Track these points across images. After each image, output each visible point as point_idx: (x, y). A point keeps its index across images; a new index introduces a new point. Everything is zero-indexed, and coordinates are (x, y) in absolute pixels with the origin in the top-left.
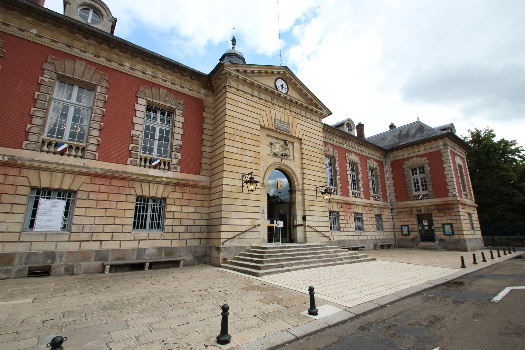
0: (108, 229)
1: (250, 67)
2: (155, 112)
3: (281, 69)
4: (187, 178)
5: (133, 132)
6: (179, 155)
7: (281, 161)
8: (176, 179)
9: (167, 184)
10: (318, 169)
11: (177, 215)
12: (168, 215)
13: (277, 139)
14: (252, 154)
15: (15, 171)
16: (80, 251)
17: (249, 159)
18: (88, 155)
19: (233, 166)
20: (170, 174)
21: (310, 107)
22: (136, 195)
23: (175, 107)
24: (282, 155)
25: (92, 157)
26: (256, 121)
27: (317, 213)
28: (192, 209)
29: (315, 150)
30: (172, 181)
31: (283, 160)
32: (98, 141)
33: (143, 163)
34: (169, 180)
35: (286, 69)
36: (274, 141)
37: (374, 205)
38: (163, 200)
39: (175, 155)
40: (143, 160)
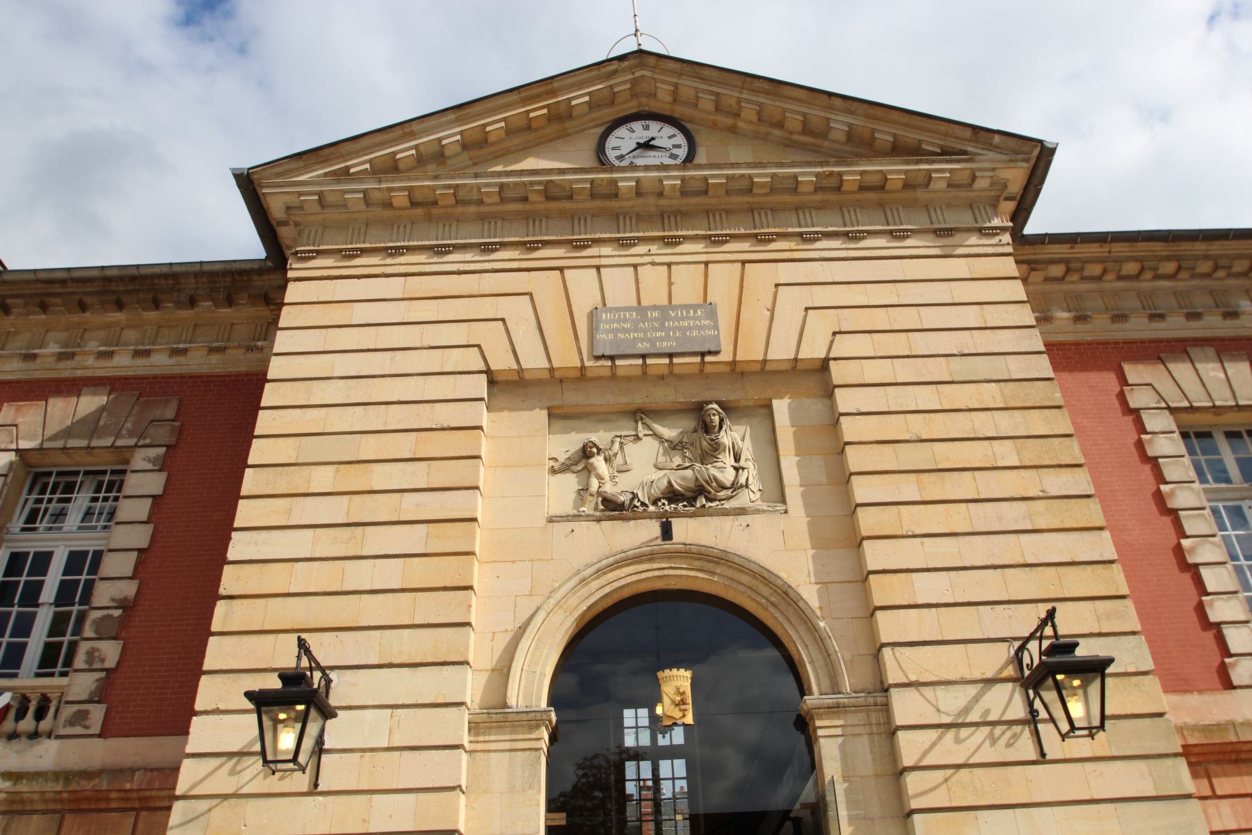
1: (413, 135)
2: (70, 488)
3: (615, 72)
6: (111, 651)
7: (667, 533)
8: (57, 775)
10: (1013, 515)
17: (390, 574)
19: (271, 637)
21: (852, 173)
23: (132, 442)
24: (672, 495)
26: (454, 360)
30: (36, 786)
31: (678, 526)
34: (23, 787)
35: (642, 66)
39: (91, 655)
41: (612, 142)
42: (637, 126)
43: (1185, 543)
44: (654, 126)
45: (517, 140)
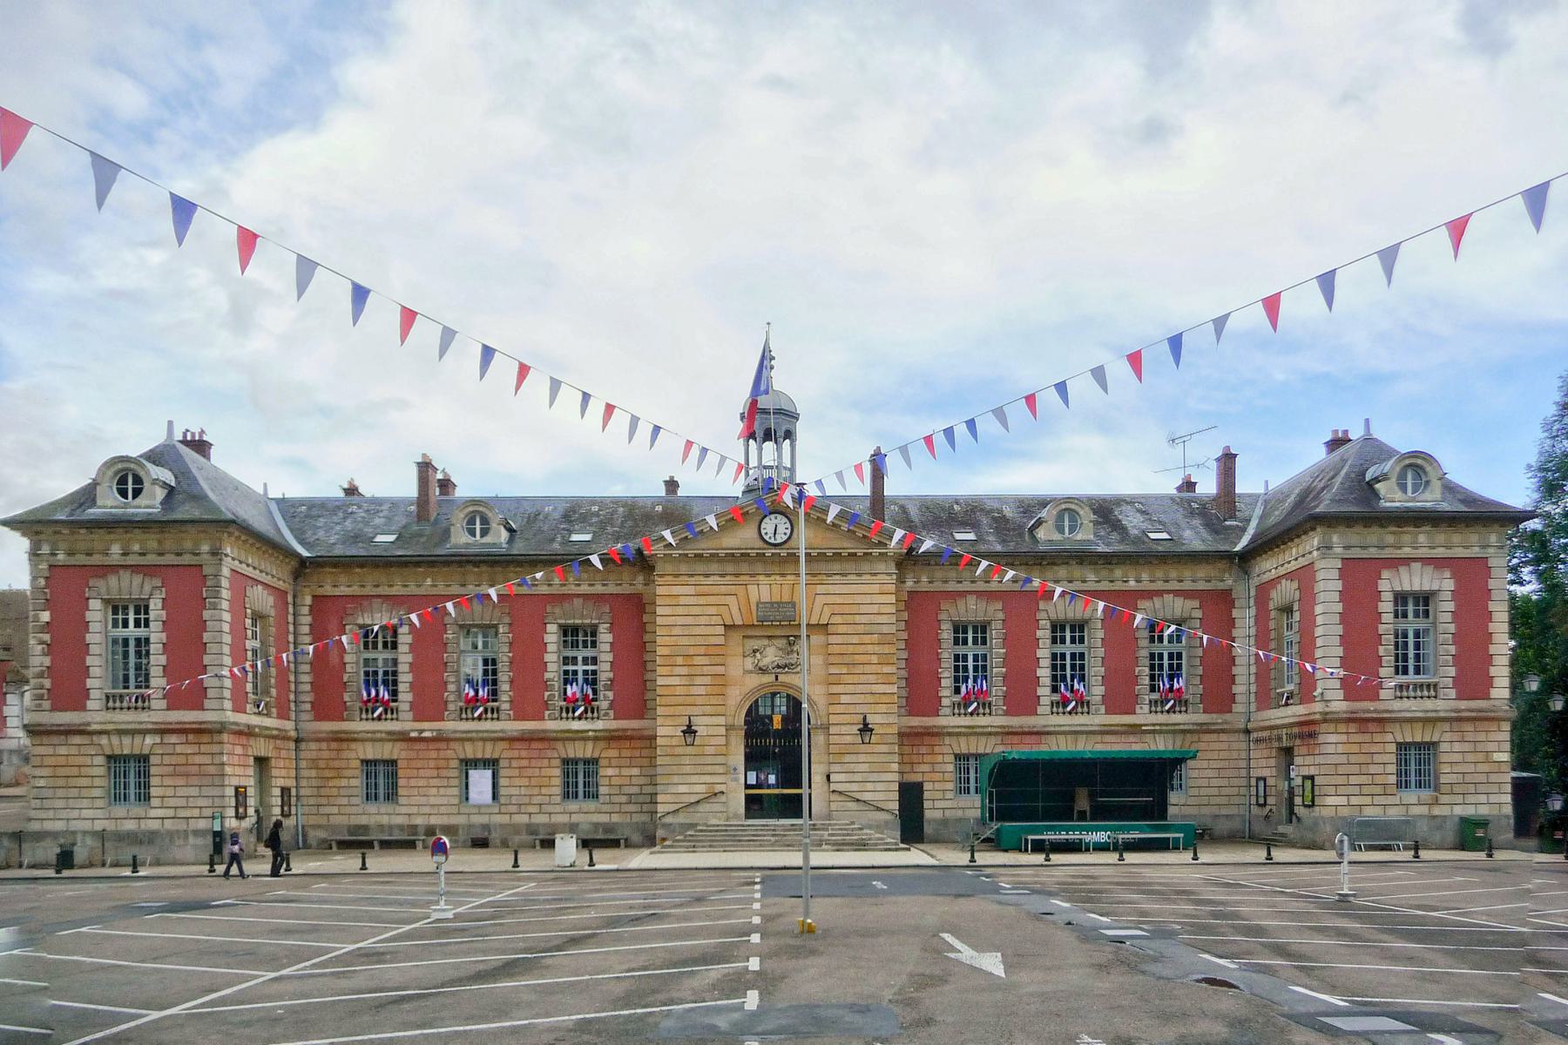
0: (536, 800)
4: (625, 727)
5: (547, 676)
6: (610, 694)
7: (777, 679)
9: (596, 739)
10: (872, 678)
11: (615, 781)
12: (602, 781)
13: (769, 637)
14: (708, 680)
15: (443, 745)
16: (510, 825)
17: (702, 691)
18: (502, 716)
20: (599, 725)
22: (560, 758)
24: (778, 667)
25: (507, 717)
26: (715, 620)
27: (864, 767)
28: (636, 771)
29: (867, 639)
31: (781, 678)
32: (510, 696)
33: (564, 715)
34: (597, 734)
36: (756, 644)
37: (1143, 728)
38: (594, 761)
39: (604, 695)
40: (564, 710)
41: (763, 526)
42: (773, 516)
43: (940, 670)
44: (779, 517)
45: (729, 524)
